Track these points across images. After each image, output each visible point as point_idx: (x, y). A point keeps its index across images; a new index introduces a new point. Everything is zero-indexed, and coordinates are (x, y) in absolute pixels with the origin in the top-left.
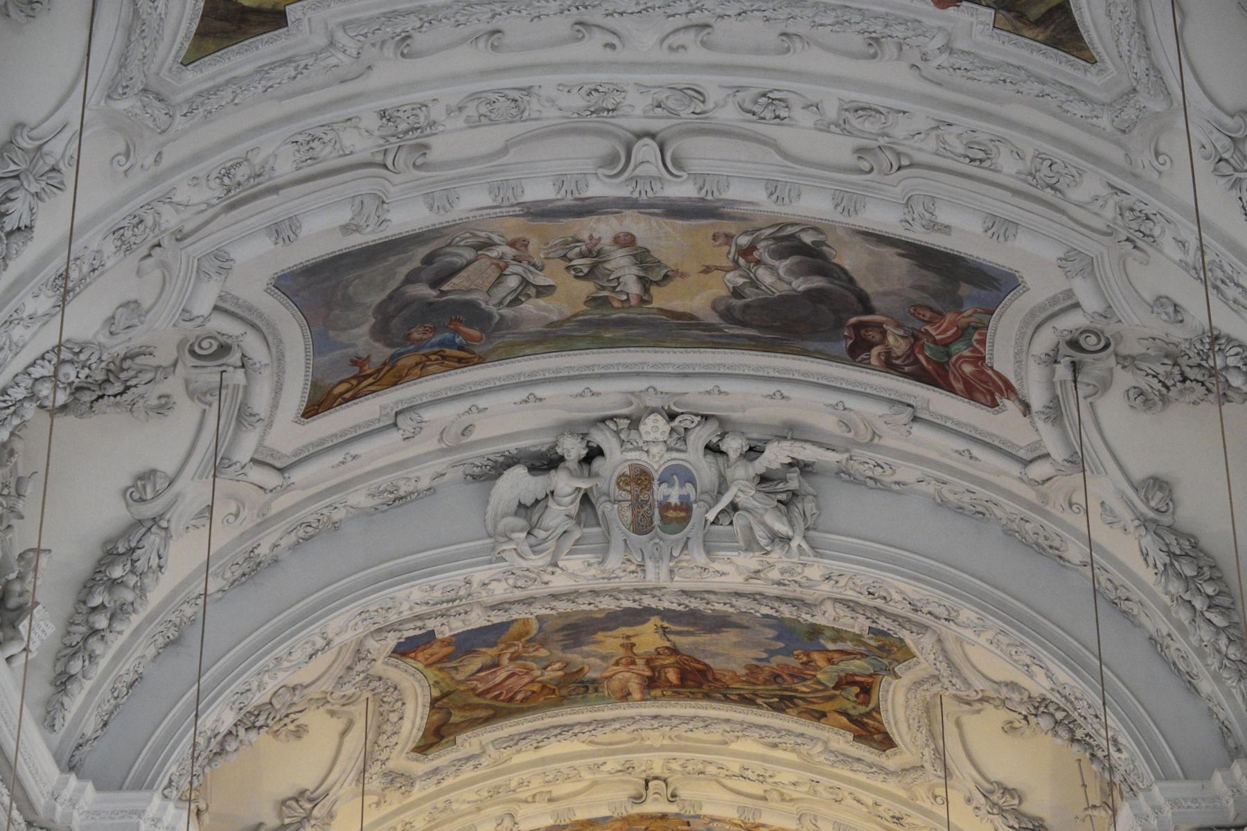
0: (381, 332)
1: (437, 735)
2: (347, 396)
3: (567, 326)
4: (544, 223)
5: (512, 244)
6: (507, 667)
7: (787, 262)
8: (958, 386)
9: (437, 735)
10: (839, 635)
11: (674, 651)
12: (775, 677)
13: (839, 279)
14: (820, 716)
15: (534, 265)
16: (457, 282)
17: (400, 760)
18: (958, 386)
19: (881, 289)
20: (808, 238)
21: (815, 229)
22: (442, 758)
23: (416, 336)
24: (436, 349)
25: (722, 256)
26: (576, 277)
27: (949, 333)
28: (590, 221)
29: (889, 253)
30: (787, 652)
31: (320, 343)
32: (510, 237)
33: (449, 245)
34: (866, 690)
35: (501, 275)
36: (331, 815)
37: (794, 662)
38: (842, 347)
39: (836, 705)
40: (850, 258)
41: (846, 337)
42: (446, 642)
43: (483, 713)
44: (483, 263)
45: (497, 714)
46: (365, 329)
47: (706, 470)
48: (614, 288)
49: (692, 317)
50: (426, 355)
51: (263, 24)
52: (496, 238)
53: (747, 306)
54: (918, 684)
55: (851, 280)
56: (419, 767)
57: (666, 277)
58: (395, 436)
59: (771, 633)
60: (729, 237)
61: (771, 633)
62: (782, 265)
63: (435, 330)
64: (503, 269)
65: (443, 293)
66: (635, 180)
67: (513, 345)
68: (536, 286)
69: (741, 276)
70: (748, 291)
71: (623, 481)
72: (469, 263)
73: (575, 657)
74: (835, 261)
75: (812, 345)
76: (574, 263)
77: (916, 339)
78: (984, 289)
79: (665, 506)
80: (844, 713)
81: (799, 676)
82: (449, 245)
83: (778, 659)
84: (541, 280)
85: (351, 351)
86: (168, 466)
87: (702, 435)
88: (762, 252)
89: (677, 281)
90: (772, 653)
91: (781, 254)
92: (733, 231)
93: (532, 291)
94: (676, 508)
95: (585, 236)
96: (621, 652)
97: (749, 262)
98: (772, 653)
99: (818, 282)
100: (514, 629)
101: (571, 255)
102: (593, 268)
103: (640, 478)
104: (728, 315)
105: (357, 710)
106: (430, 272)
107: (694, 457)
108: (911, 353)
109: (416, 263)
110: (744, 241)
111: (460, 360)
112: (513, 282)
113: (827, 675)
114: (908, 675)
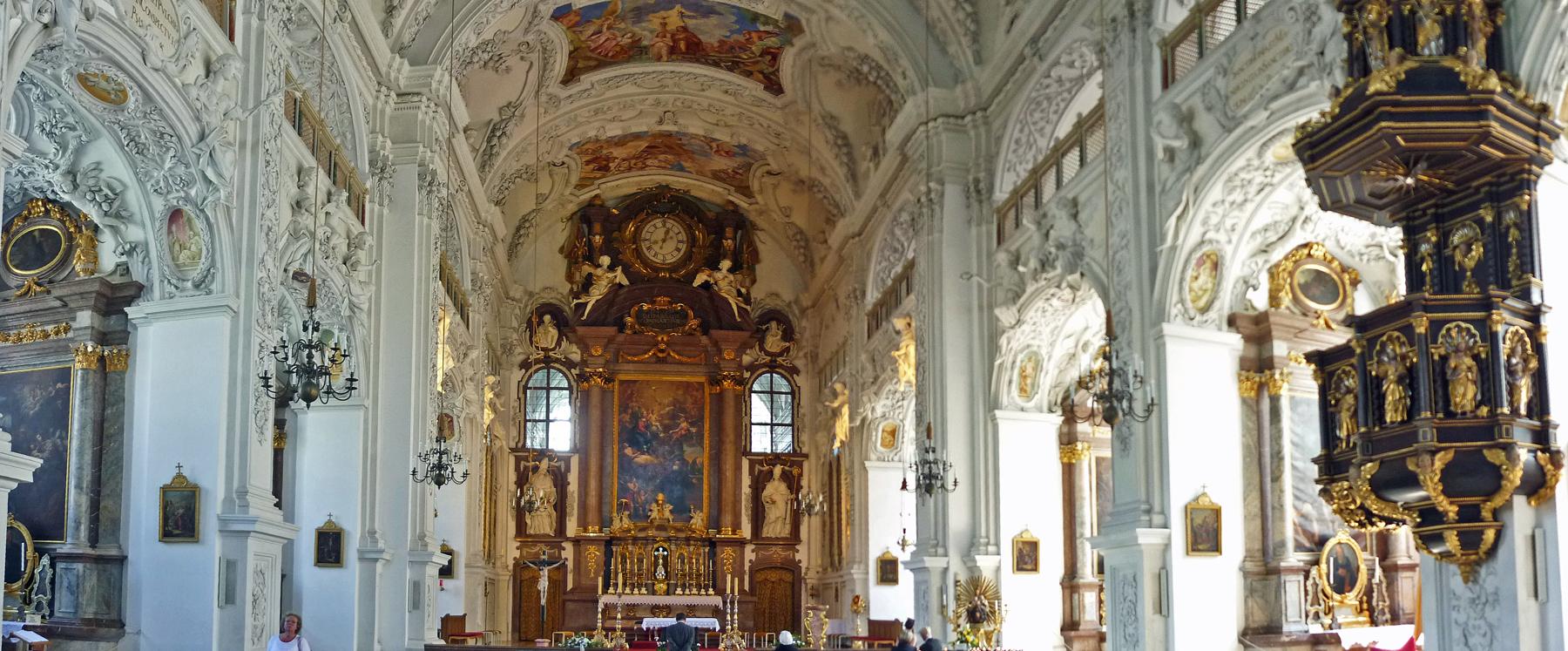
1: (571, 76)
6: (606, 34)
9: (571, 76)
10: (767, 20)
11: (685, 29)
12: (732, 48)
14: (749, 74)
17: (554, 88)
22: (574, 89)
30: (739, 32)
34: (774, 56)
36: (523, 116)
37: (742, 39)
39: (758, 67)
42: (577, 13)
43: (593, 63)
45: (601, 64)
54: (803, 49)
56: (563, 93)
59: (733, 18)
61: (733, 18)
73: (636, 29)
80: (761, 72)
81: (743, 48)
83: (735, 36)
90: (732, 32)
96: (659, 29)
98: (732, 32)
100: (610, 8)
105: (534, 57)
113: (756, 49)
114: (799, 42)
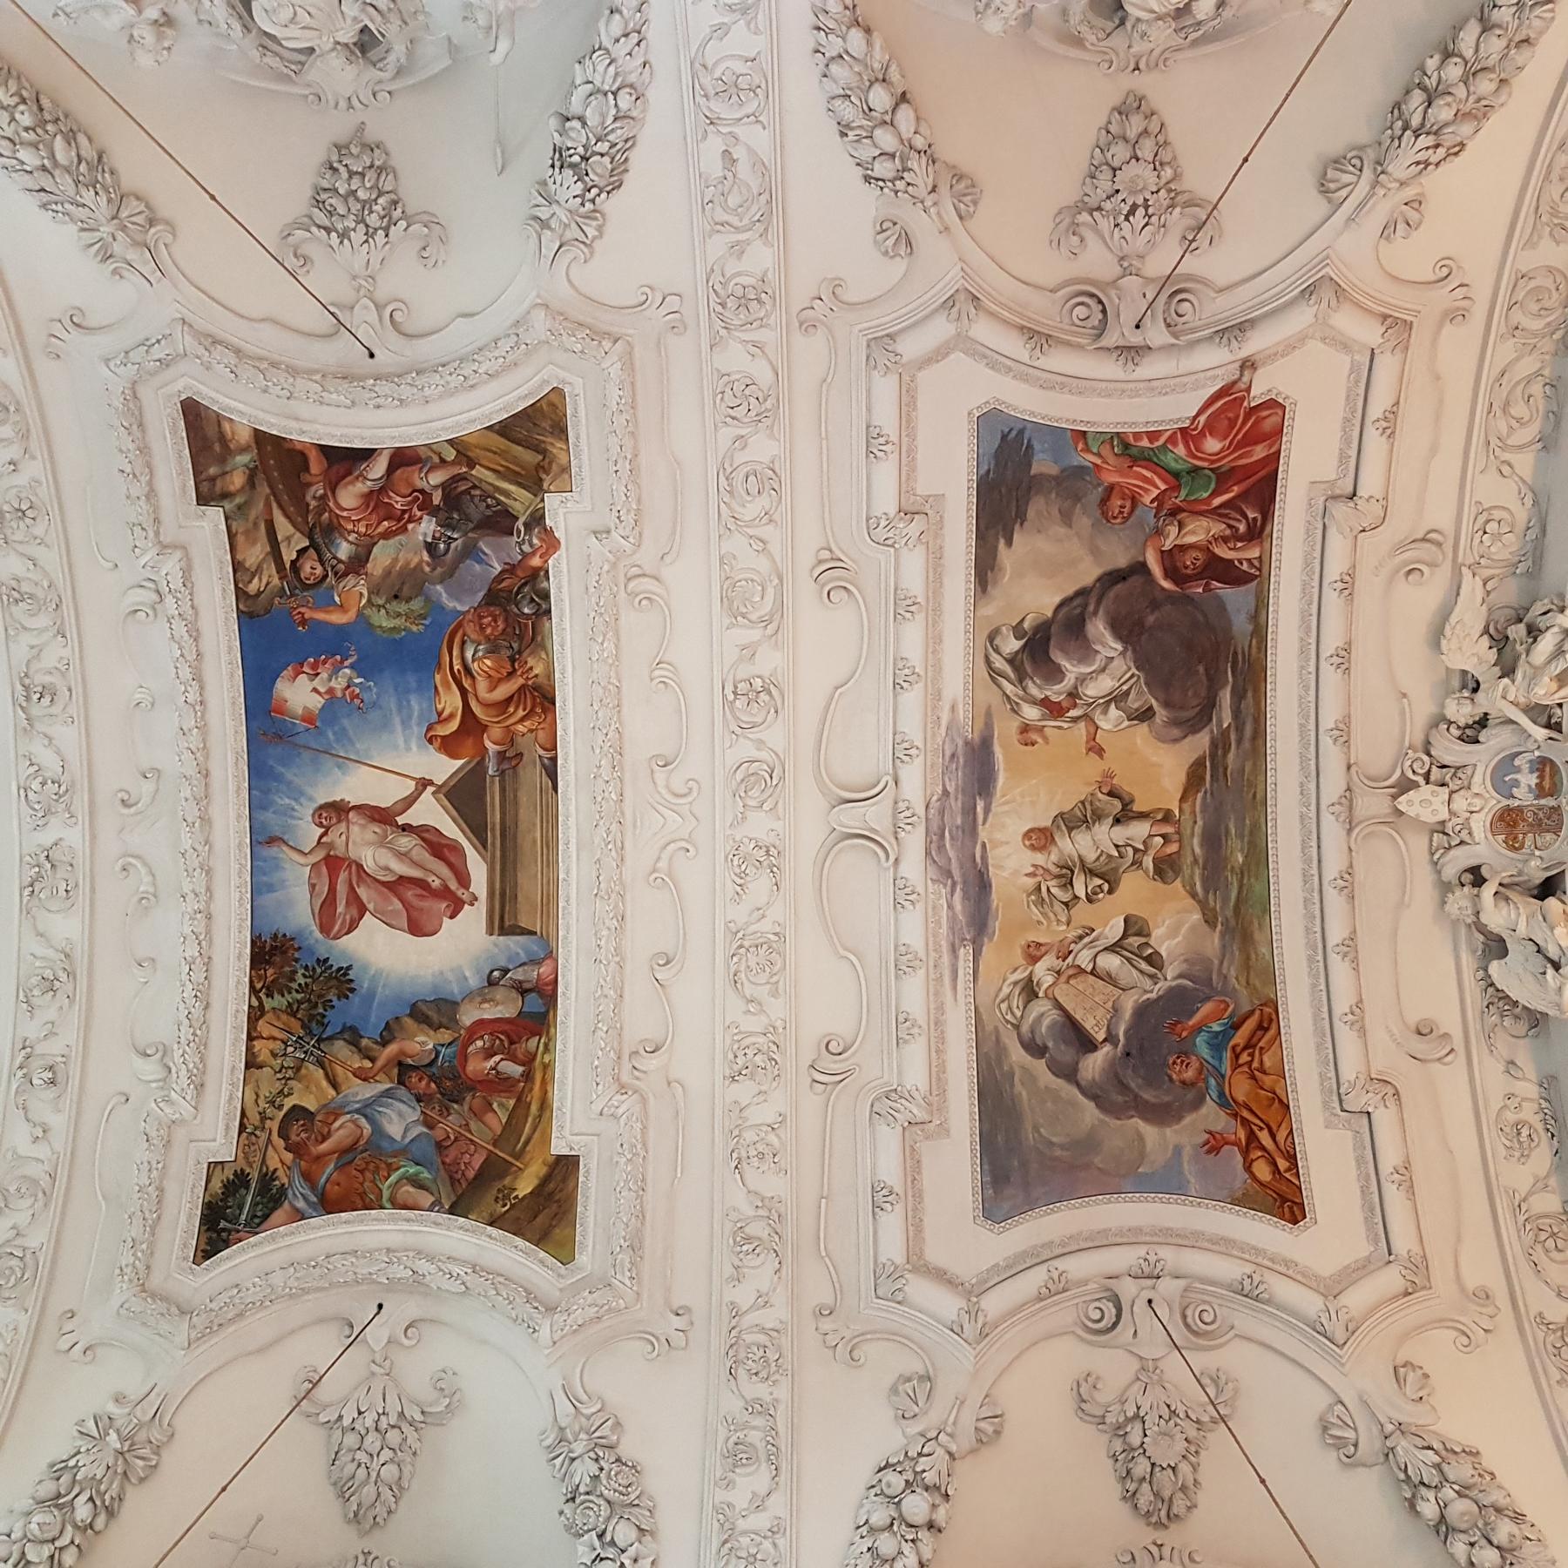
0: (1161, 1114)
2: (1282, 1164)
3: (1214, 902)
4: (997, 925)
5: (1034, 960)
7: (1065, 663)
8: (1260, 452)
13: (1085, 606)
15: (1081, 938)
16: (1095, 1026)
18: (1260, 452)
19: (1088, 559)
20: (1012, 645)
21: (991, 638)
23: (1189, 1074)
24: (1228, 1055)
25: (1067, 736)
26: (1110, 892)
27: (1148, 474)
28: (996, 877)
29: (1007, 557)
31: (1167, 1183)
32: (1019, 958)
33: (1017, 1027)
35: (1093, 973)
38: (1235, 598)
40: (1038, 598)
41: (1207, 588)
44: (1062, 994)
46: (1150, 1132)
47: (1495, 741)
48: (1136, 850)
49: (1199, 764)
50: (1236, 1066)
51: (564, 1180)
52: (1020, 975)
53: (1167, 704)
55: (1082, 593)
57: (1111, 794)
58: (1384, 1119)
60: (1025, 729)
62: (1072, 670)
63: (1185, 1053)
64: (1082, 971)
65: (1110, 1038)
66: (896, 830)
67: (1247, 966)
68: (1125, 936)
69: (1105, 712)
70: (1134, 703)
71: (1513, 844)
72: (1058, 1006)
74: (1050, 614)
75: (1240, 624)
76: (1082, 895)
77: (1174, 512)
78: (1030, 446)
79: (1541, 791)
82: (1017, 1027)
84: (1114, 930)
85: (1187, 1152)
86: (1322, 1400)
87: (1449, 749)
88: (1056, 693)
89: (1123, 783)
91: (1056, 674)
92: (1015, 724)
93: (1134, 941)
94: (1541, 777)
95: (1031, 882)
97: (1075, 706)
99: (1098, 628)
101: (1065, 896)
102: (1090, 872)
103: (1509, 822)
104: (1192, 725)
106: (1066, 1054)
107: (1483, 757)
108: (1217, 513)
109: (1040, 1066)
110: (1031, 713)
111: (1262, 1028)
112: (1111, 962)
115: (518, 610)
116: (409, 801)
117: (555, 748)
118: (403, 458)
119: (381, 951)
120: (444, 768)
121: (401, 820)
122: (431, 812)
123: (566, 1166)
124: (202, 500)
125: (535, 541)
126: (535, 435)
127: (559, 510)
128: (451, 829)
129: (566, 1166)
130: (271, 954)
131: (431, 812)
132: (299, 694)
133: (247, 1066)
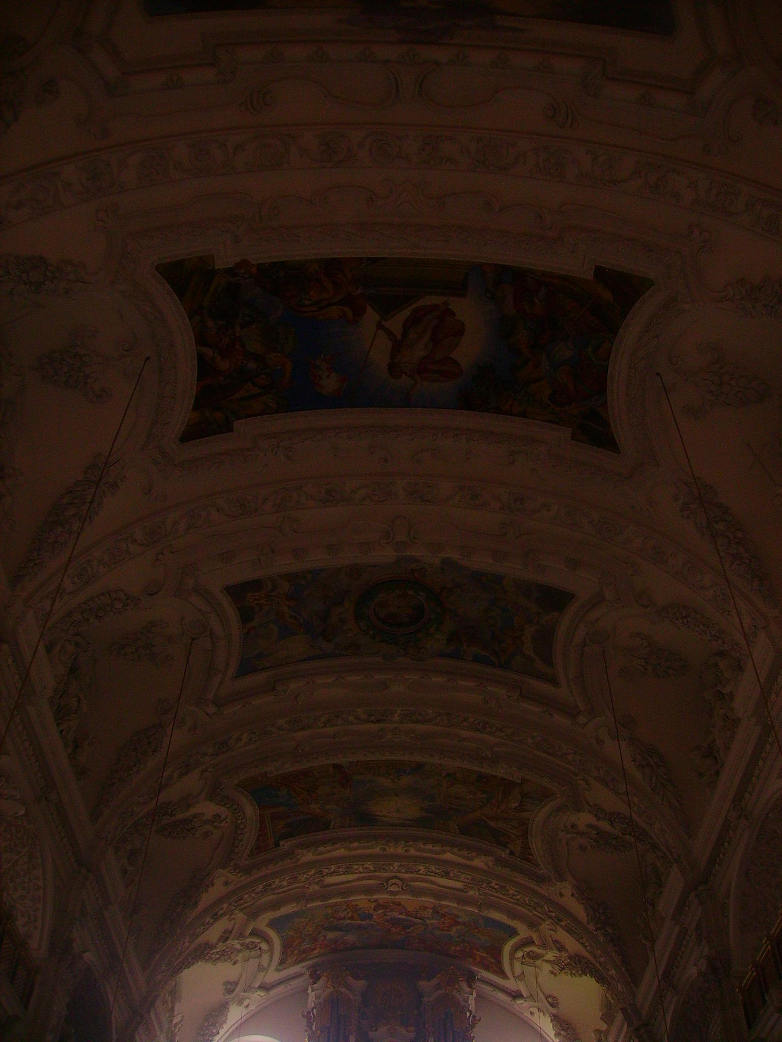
115: (283, 278)
116: (389, 333)
117: (361, 258)
118: (201, 340)
119: (469, 350)
120: (371, 316)
121: (399, 337)
122: (396, 323)
123: (599, 272)
124: (230, 430)
125: (242, 271)
126: (184, 277)
127: (225, 260)
128: (406, 313)
129: (599, 272)
130: (468, 402)
131: (396, 323)
132: (330, 383)
133: (525, 416)
